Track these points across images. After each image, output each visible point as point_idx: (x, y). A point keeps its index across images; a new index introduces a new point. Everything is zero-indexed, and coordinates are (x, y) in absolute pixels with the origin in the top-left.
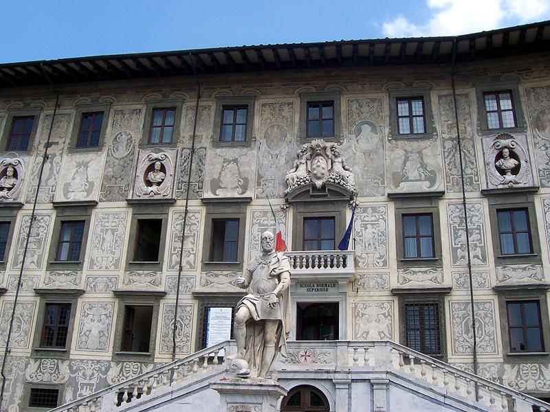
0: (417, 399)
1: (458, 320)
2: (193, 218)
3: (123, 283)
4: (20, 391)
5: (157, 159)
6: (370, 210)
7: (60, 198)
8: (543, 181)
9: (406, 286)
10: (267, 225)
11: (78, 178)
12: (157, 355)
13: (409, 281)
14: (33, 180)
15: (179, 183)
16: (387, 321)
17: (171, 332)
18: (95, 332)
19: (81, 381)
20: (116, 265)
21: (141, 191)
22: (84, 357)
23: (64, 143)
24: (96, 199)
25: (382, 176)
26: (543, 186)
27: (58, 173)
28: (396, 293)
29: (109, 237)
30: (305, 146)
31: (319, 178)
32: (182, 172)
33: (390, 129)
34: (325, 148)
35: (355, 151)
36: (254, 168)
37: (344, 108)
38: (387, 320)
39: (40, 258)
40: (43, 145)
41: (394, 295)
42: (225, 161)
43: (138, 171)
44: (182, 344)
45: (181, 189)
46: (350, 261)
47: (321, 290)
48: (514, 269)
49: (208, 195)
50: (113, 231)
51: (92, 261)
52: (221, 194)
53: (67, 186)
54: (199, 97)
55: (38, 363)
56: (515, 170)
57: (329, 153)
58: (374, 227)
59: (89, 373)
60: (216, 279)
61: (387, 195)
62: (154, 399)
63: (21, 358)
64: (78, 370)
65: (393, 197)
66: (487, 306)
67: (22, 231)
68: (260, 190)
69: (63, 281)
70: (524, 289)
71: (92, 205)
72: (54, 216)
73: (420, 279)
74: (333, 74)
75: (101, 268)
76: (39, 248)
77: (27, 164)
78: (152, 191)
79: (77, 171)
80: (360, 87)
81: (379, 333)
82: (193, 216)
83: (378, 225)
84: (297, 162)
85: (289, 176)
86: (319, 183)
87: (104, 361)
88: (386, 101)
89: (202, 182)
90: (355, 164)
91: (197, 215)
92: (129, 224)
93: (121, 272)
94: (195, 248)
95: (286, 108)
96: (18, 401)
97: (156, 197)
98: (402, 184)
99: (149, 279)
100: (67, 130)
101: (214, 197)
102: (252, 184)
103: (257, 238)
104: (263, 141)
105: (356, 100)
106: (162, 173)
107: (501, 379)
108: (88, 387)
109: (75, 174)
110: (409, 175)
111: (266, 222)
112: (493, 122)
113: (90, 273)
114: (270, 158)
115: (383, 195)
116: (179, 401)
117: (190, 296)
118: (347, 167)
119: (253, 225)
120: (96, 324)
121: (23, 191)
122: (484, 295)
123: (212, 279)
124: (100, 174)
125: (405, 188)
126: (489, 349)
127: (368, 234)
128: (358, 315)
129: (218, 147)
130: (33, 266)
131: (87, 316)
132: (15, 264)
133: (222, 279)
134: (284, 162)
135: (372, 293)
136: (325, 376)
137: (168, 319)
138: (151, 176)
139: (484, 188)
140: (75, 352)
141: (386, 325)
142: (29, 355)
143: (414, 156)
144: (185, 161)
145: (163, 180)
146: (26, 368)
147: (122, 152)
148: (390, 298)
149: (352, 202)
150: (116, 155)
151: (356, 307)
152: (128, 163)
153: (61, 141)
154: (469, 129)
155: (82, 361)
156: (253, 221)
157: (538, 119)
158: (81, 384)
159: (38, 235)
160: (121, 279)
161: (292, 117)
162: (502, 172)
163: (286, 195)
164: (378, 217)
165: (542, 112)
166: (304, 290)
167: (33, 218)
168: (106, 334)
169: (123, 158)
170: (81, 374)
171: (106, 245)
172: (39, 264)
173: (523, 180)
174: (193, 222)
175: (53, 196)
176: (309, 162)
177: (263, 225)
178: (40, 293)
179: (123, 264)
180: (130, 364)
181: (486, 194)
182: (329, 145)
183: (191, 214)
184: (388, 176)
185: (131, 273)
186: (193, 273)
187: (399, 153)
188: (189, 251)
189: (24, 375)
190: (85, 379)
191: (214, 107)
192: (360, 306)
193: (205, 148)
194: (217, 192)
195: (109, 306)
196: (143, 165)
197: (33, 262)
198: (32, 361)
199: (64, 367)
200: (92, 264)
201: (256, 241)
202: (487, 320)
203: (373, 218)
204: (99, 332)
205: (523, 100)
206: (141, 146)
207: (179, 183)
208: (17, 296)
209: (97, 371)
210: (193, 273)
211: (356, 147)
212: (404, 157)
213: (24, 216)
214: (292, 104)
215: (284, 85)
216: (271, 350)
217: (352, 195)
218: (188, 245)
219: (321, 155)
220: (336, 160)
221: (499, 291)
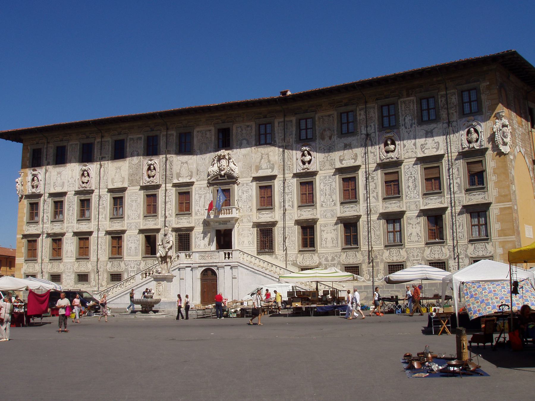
0: (248, 272)
1: (280, 235)
4: (105, 276)
5: (151, 164)
6: (245, 185)
7: (111, 187)
8: (321, 168)
11: (117, 176)
16: (252, 237)
18: (133, 248)
19: (130, 269)
20: (139, 217)
21: (145, 181)
24: (126, 186)
25: (251, 167)
26: (321, 170)
29: (134, 204)
31: (222, 171)
34: (224, 156)
36: (195, 166)
37: (234, 131)
42: (182, 163)
48: (305, 211)
49: (175, 181)
50: (136, 201)
51: (128, 215)
54: (167, 129)
56: (309, 162)
57: (227, 157)
58: (245, 194)
59: (133, 266)
60: (181, 221)
63: (104, 261)
65: (256, 179)
66: (293, 228)
68: (198, 177)
69: (117, 226)
70: (307, 220)
73: (265, 217)
74: (229, 113)
76: (104, 211)
80: (242, 119)
85: (209, 170)
88: (254, 126)
91: (171, 191)
92: (142, 197)
93: (141, 220)
95: (208, 133)
96: (105, 280)
97: (153, 184)
98: (260, 171)
99: (153, 223)
101: (178, 182)
102: (194, 174)
105: (241, 127)
107: (296, 261)
112: (303, 137)
120: (133, 244)
122: (290, 223)
123: (179, 221)
124: (127, 173)
125: (261, 173)
126: (292, 248)
127: (244, 197)
133: (184, 221)
136: (215, 264)
139: (295, 172)
140: (126, 258)
143: (265, 157)
150: (133, 162)
153: (107, 156)
154: (291, 140)
155: (129, 261)
157: (322, 133)
161: (211, 138)
162: (304, 163)
165: (325, 130)
166: (218, 224)
172: (106, 218)
173: (312, 168)
179: (142, 217)
181: (296, 175)
182: (227, 152)
184: (253, 168)
186: (171, 219)
191: (175, 134)
192: (241, 230)
196: (146, 167)
198: (109, 262)
199: (122, 264)
200: (128, 217)
202: (292, 235)
205: (317, 123)
210: (171, 219)
214: (210, 130)
215: (207, 120)
216: (169, 264)
217: (236, 179)
219: (223, 159)
221: (297, 222)
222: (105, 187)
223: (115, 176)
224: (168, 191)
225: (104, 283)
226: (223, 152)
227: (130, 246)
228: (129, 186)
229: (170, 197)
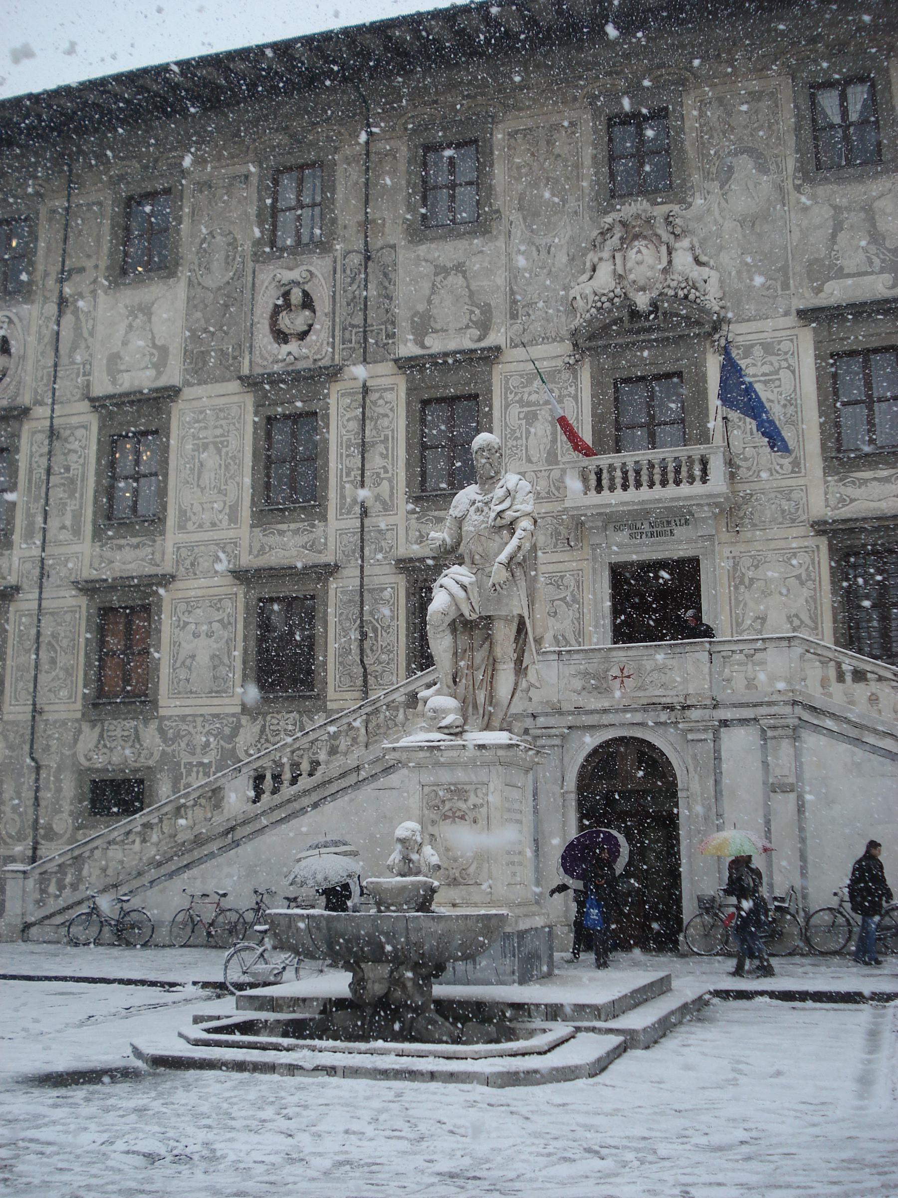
2: (381, 402)
3: (250, 553)
4: (69, 788)
6: (758, 351)
7: (102, 387)
9: (846, 512)
10: (537, 403)
12: (331, 693)
13: (852, 501)
14: (42, 353)
15: (344, 329)
16: (806, 592)
17: (354, 647)
18: (203, 659)
19: (185, 758)
22: (188, 711)
23: (96, 267)
27: (92, 334)
28: (821, 528)
30: (609, 219)
32: (348, 305)
33: (797, 160)
35: (721, 221)
36: (500, 279)
38: (805, 590)
39: (77, 516)
40: (51, 282)
41: (820, 533)
42: (442, 271)
43: (258, 311)
44: (379, 668)
45: (351, 342)
46: (717, 467)
47: (659, 534)
49: (408, 349)
51: (182, 513)
52: (435, 344)
53: (114, 359)
55: (97, 730)
61: (794, 313)
62: (324, 784)
63: (64, 723)
64: (178, 736)
67: (35, 465)
68: (517, 327)
69: (128, 560)
71: (171, 393)
72: (95, 429)
75: (200, 526)
77: (27, 323)
78: (289, 353)
79: (130, 326)
81: (789, 617)
82: (381, 397)
83: (777, 383)
84: (591, 257)
86: (642, 301)
87: (227, 715)
89: (393, 323)
90: (721, 248)
91: (388, 396)
93: (243, 531)
94: (389, 467)
96: (67, 807)
97: (300, 365)
100: (96, 237)
102: (499, 317)
103: (518, 434)
104: (516, 216)
106: (307, 313)
108: (201, 769)
109: (132, 333)
110: (845, 263)
111: (534, 397)
113: (181, 537)
114: (535, 253)
115: (787, 314)
116: (373, 786)
117: (387, 569)
118: (703, 259)
119: (507, 406)
120: (203, 642)
121: (27, 379)
125: (836, 292)
128: (742, 582)
129: (421, 242)
130: (64, 536)
131: (184, 628)
132: (29, 534)
134: (565, 259)
135: (770, 534)
137: (347, 619)
138: (285, 322)
140: (169, 704)
141: (801, 601)
142: (79, 715)
143: (855, 218)
144: (353, 279)
145: (310, 326)
146: (76, 741)
147: (218, 277)
148: (811, 542)
149: (716, 336)
150: (208, 282)
151: (735, 565)
152: (234, 297)
155: (183, 718)
156: (506, 398)
158: (185, 765)
159: (68, 469)
160: (245, 543)
163: (574, 334)
164: (776, 365)
167: (53, 434)
168: (226, 661)
169: (220, 288)
170: (183, 745)
171: (208, 477)
172: (77, 531)
174: (381, 410)
175: (88, 386)
176: (618, 255)
177: (529, 404)
178: (89, 588)
180: (279, 717)
183: (377, 395)
185: (265, 530)
187: (822, 214)
188: (378, 474)
189: (74, 755)
190: (194, 754)
192: (746, 562)
193: (393, 247)
194: (428, 341)
195: (227, 603)
197: (64, 527)
198: (86, 727)
199: (150, 735)
201: (516, 439)
203: (766, 369)
204: (213, 657)
206: (257, 257)
207: (344, 329)
208: (40, 599)
209: (216, 736)
211: (721, 211)
212: (830, 223)
213: (34, 433)
218: (375, 462)
220: (677, 245)
222: (78, 394)
223: (125, 343)
224: (374, 396)
225: (63, 823)
226: (634, 208)
227: (187, 647)
228: (188, 384)
229: (385, 422)
